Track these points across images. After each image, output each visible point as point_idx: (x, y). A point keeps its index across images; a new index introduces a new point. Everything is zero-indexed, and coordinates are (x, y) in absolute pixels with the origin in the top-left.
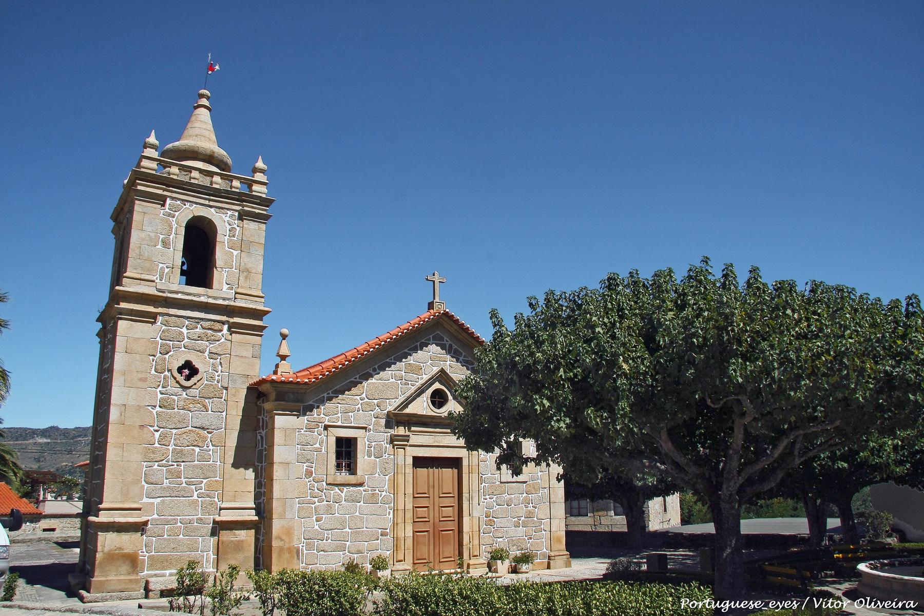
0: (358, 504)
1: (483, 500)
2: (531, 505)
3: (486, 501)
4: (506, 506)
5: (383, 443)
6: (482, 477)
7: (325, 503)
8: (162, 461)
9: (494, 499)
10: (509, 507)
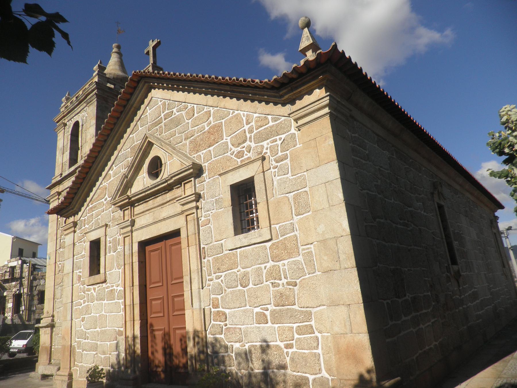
0: (104, 302)
1: (208, 282)
2: (284, 281)
3: (211, 283)
4: (240, 288)
5: (117, 236)
6: (204, 248)
7: (86, 303)
8: (61, 282)
9: (222, 278)
10: (245, 289)
